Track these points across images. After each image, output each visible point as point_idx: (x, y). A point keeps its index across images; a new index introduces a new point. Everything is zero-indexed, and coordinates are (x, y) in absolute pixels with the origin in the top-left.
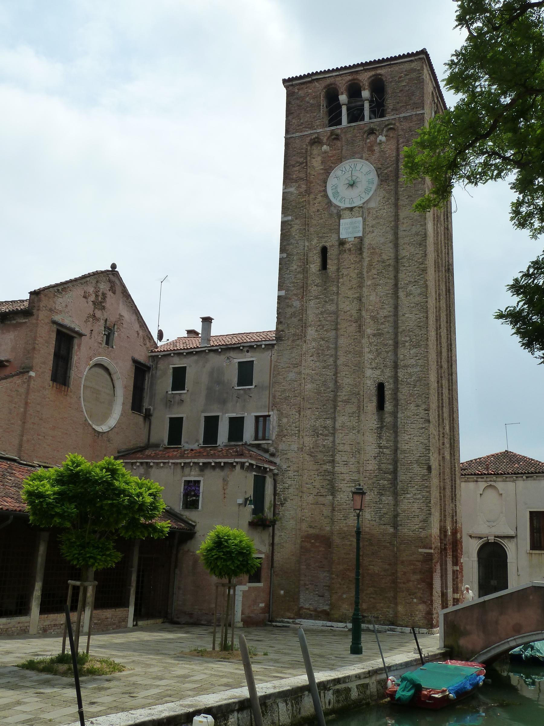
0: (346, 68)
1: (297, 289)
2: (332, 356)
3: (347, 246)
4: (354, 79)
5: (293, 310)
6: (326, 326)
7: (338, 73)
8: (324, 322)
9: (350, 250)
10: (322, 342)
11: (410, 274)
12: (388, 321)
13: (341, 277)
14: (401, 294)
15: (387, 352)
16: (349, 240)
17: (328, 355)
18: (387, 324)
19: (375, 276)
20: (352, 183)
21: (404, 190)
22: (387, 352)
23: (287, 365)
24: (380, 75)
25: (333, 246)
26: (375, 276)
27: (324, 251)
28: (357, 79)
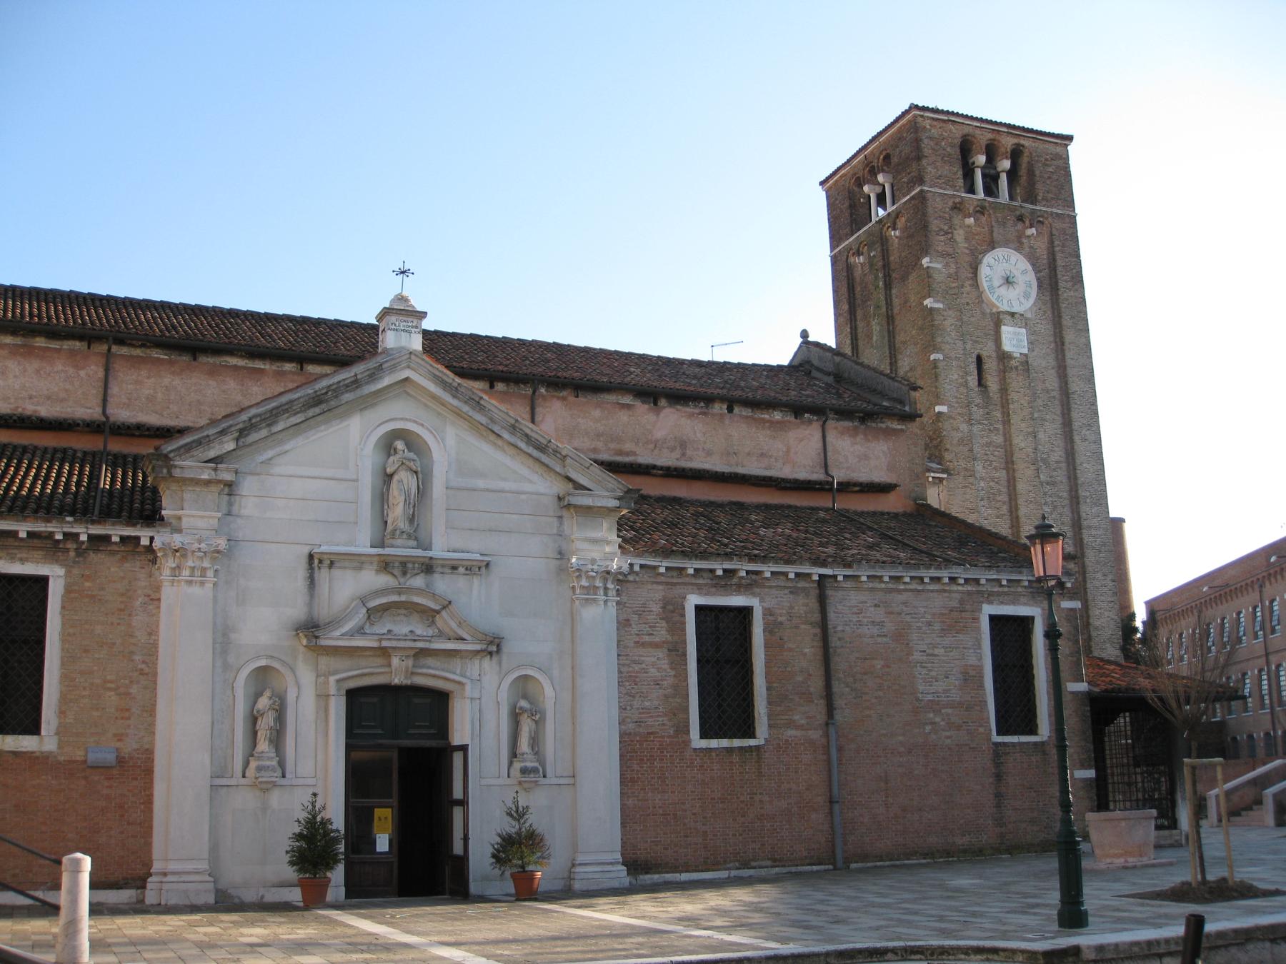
0: (991, 122)
1: (962, 407)
2: (1004, 503)
3: (1013, 363)
4: (994, 140)
5: (960, 435)
6: (994, 463)
7: (978, 125)
8: (991, 458)
9: (1016, 368)
10: (992, 484)
11: (1083, 414)
12: (1060, 468)
13: (1010, 401)
14: (1077, 438)
15: (1063, 507)
16: (1015, 355)
17: (1000, 501)
18: (1060, 472)
19: (1041, 408)
20: (1011, 280)
21: (1065, 307)
22: (1063, 507)
23: (961, 509)
24: (1023, 146)
25: (989, 357)
26: (1041, 408)
27: (979, 359)
28: (999, 141)
